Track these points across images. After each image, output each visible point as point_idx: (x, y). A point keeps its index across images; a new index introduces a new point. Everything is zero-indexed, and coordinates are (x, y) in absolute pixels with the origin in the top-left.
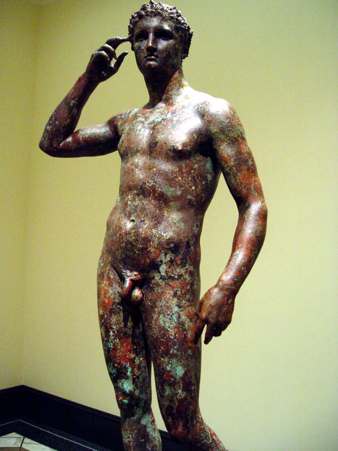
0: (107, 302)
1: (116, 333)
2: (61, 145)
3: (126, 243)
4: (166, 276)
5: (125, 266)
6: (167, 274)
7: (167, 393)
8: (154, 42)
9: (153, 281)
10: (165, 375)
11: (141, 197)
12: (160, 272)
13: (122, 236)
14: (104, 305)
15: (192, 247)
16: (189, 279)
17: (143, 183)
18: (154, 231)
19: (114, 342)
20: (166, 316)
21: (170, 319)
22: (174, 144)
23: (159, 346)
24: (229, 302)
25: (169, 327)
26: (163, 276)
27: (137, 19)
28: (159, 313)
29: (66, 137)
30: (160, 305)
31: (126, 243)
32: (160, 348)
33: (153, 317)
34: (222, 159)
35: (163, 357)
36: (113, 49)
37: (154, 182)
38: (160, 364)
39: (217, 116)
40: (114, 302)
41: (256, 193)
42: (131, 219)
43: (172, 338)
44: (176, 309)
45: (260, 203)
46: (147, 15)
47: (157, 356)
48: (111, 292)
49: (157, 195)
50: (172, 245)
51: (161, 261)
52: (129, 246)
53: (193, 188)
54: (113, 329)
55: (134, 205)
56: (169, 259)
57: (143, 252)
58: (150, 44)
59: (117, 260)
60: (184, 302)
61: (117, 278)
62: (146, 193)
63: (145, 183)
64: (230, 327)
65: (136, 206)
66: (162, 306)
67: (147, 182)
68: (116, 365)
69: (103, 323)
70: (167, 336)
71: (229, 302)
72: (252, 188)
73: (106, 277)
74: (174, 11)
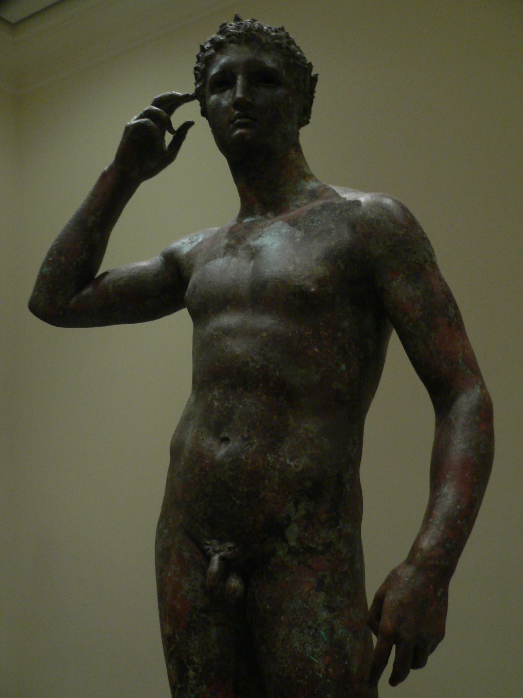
1: (200, 670)
2: (72, 302)
8: (246, 90)
12: (286, 541)
15: (347, 486)
16: (345, 551)
18: (270, 458)
19: (196, 692)
20: (306, 631)
21: (313, 636)
22: (302, 283)
24: (439, 594)
25: (313, 654)
27: (212, 51)
29: (79, 289)
36: (165, 114)
39: (382, 224)
41: (469, 371)
42: (222, 436)
43: (321, 676)
44: (325, 614)
45: (479, 390)
46: (231, 42)
48: (186, 586)
49: (272, 384)
50: (308, 484)
51: (288, 518)
53: (343, 367)
54: (194, 663)
56: (303, 512)
58: (239, 95)
60: (339, 598)
63: (247, 363)
64: (441, 646)
67: (249, 360)
71: (439, 594)
72: (460, 360)
74: (282, 34)
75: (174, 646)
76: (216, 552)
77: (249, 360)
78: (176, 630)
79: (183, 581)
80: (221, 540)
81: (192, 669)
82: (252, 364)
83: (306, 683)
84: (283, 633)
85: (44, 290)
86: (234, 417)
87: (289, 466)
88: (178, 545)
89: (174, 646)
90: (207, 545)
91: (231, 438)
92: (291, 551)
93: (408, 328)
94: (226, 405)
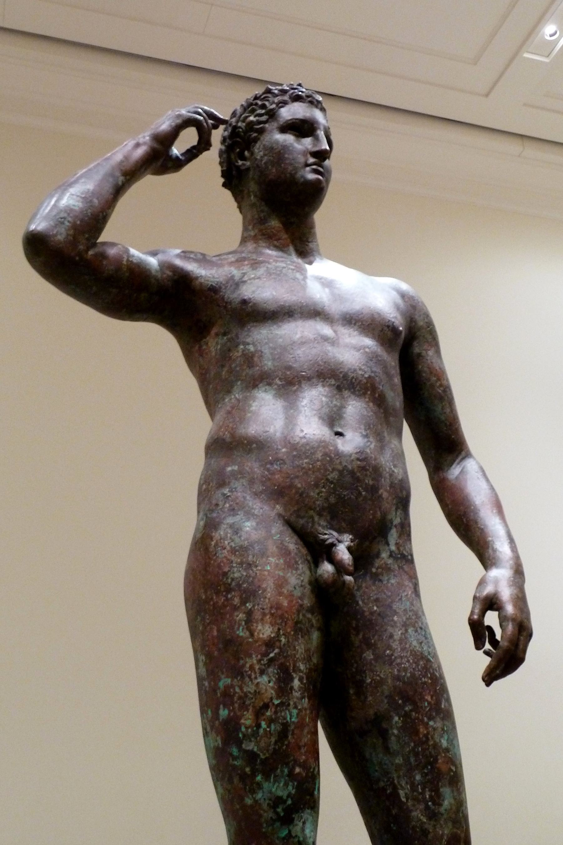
0: (285, 604)
3: (341, 472)
4: (397, 552)
5: (334, 523)
6: (398, 549)
7: (446, 803)
9: (377, 563)
10: (440, 761)
11: (346, 393)
12: (388, 544)
13: (330, 457)
14: (280, 612)
22: (393, 320)
23: (421, 694)
28: (405, 626)
30: (403, 608)
31: (341, 472)
32: (423, 699)
33: (391, 636)
34: (431, 373)
35: (430, 719)
37: (372, 372)
38: (426, 736)
40: (301, 606)
47: (418, 718)
49: (377, 395)
52: (348, 479)
54: (300, 671)
55: (336, 406)
57: (373, 495)
59: (314, 509)
61: (304, 551)
68: (297, 770)
69: (271, 661)
70: (431, 671)
75: (277, 651)
76: (340, 542)
78: (281, 631)
79: (289, 574)
80: (340, 531)
81: (298, 678)
82: (360, 372)
83: (430, 681)
84: (400, 633)
86: (345, 415)
87: (393, 471)
88: (279, 536)
89: (277, 651)
90: (326, 534)
91: (345, 433)
92: (391, 555)
93: (440, 391)
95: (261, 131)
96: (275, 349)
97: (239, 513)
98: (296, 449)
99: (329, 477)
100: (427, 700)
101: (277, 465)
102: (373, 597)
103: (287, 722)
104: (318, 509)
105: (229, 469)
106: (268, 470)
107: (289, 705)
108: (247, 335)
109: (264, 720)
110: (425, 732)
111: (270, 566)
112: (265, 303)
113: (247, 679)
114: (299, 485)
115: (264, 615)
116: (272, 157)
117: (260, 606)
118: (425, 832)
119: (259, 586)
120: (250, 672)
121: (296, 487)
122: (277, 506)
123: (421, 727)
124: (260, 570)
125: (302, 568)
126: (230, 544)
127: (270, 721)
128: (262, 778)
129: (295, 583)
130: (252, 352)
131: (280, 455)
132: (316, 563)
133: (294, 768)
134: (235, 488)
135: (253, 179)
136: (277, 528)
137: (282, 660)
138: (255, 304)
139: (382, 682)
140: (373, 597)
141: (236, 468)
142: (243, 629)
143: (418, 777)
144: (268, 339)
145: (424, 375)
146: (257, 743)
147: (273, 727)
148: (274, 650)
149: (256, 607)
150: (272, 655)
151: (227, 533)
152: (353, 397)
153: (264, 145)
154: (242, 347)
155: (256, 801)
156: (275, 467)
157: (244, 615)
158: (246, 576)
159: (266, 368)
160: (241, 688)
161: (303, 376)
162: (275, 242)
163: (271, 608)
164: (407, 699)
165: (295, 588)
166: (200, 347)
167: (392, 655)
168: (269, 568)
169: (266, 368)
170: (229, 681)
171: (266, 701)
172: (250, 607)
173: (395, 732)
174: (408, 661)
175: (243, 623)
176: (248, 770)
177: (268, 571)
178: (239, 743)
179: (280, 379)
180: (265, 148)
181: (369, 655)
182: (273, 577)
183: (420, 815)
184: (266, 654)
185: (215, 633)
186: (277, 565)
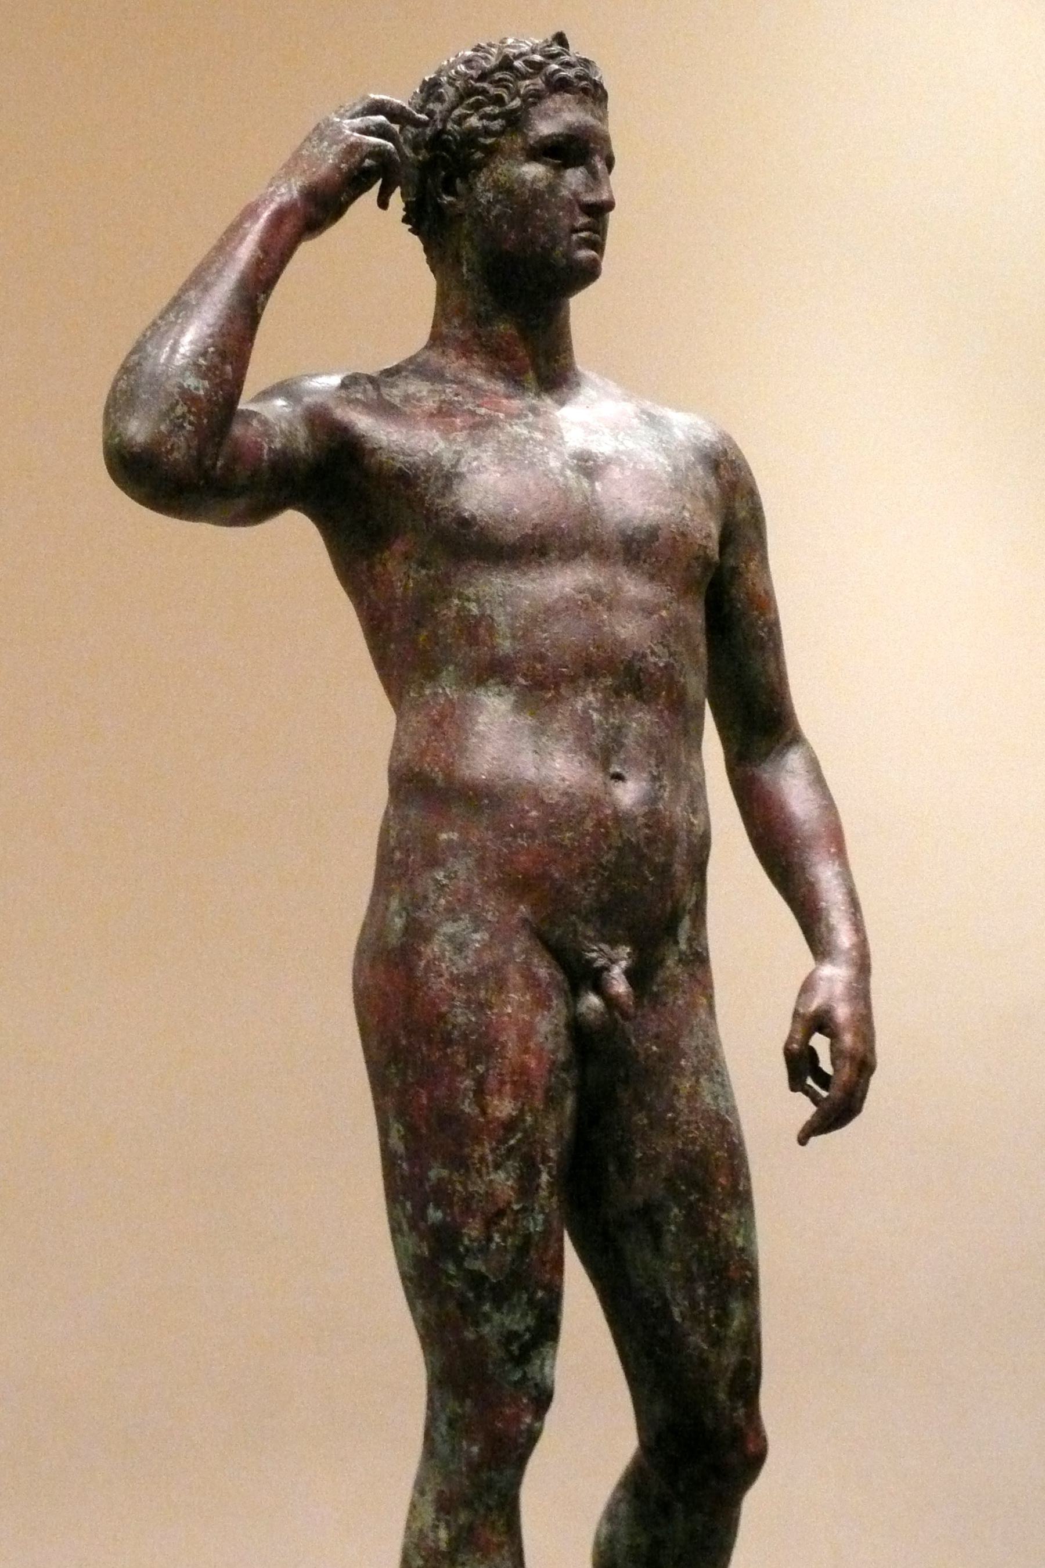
6: (691, 946)
7: (736, 1323)
9: (662, 975)
11: (629, 697)
12: (677, 943)
13: (606, 827)
17: (635, 654)
26: (684, 953)
28: (697, 1073)
30: (694, 1044)
32: (714, 1183)
33: (676, 1091)
35: (723, 1210)
37: (671, 655)
38: (716, 1234)
40: (554, 1063)
54: (549, 1159)
55: (613, 726)
59: (578, 913)
62: (647, 689)
63: (644, 656)
65: (619, 729)
66: (697, 1047)
67: (648, 651)
69: (510, 1150)
73: (515, 978)
75: (519, 1135)
77: (648, 651)
80: (613, 943)
84: (688, 1085)
85: (189, 427)
86: (626, 741)
88: (523, 956)
89: (519, 1135)
90: (593, 951)
91: (626, 775)
93: (763, 634)
94: (611, 720)
95: (491, 151)
96: (515, 617)
97: (463, 916)
98: (552, 814)
99: (604, 861)
100: (721, 1184)
101: (522, 837)
102: (653, 1028)
103: (530, 1233)
104: (584, 912)
105: (444, 836)
106: (508, 846)
107: (533, 1210)
108: (465, 582)
109: (498, 1231)
110: (716, 1229)
111: (512, 1007)
112: (501, 529)
113: (474, 1175)
114: (557, 875)
115: (502, 1083)
116: (511, 209)
117: (497, 1070)
118: (704, 1363)
119: (496, 1040)
120: (478, 1166)
121: (551, 877)
122: (522, 907)
123: (711, 1222)
124: (496, 1014)
125: (557, 1005)
126: (450, 969)
127: (505, 1234)
128: (491, 1308)
129: (548, 1030)
130: (475, 617)
131: (528, 822)
132: (575, 992)
133: (535, 1292)
134: (456, 872)
135: (469, 236)
136: (521, 944)
137: (524, 1149)
138: (482, 529)
139: (657, 1159)
140: (653, 1028)
141: (455, 836)
142: (470, 1104)
143: (701, 1291)
144: (503, 596)
145: (739, 606)
146: (486, 1262)
147: (510, 1240)
148: (514, 1135)
149: (491, 1072)
150: (512, 1142)
151: (445, 950)
152: (638, 704)
153: (496, 182)
154: (456, 601)
155: (481, 1338)
156: (519, 841)
157: (472, 1083)
158: (476, 1023)
159: (501, 653)
160: (465, 1187)
161: (562, 674)
162: (505, 365)
163: (513, 1073)
164: (694, 1184)
165: (546, 1038)
166: (371, 567)
167: (674, 1119)
168: (510, 1011)
169: (501, 653)
170: (445, 1173)
171: (501, 1205)
172: (481, 1071)
173: (673, 1228)
174: (698, 1128)
175: (471, 1095)
176: (471, 1295)
177: (509, 1015)
178: (459, 1260)
179: (525, 676)
180: (497, 186)
181: (641, 1119)
182: (516, 1025)
183: (699, 1341)
184: (503, 1141)
185: (425, 1101)
186: (521, 1005)
